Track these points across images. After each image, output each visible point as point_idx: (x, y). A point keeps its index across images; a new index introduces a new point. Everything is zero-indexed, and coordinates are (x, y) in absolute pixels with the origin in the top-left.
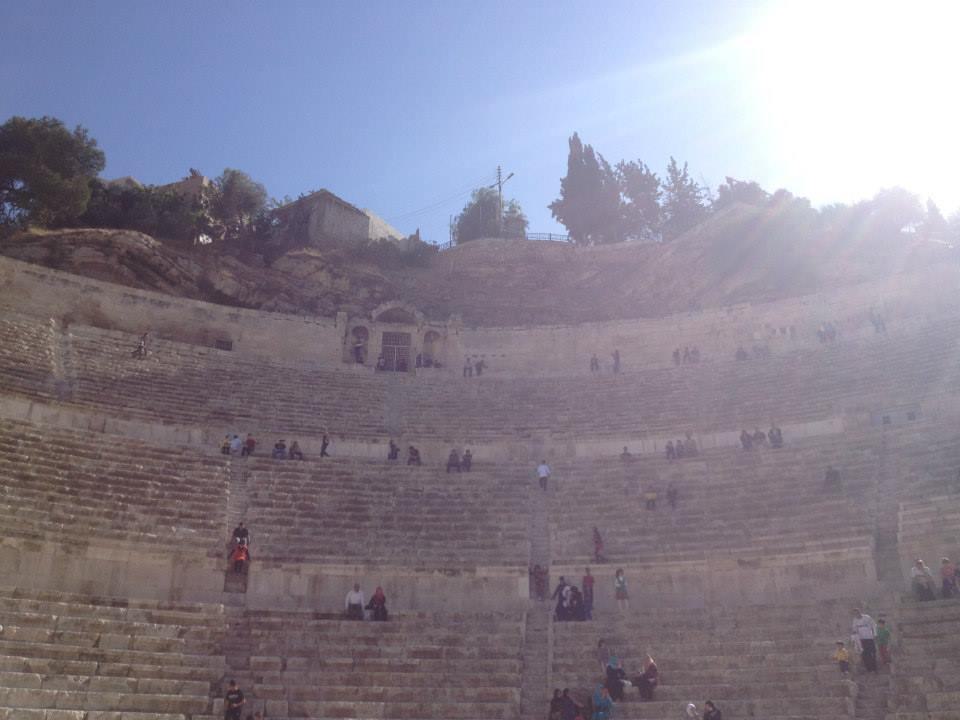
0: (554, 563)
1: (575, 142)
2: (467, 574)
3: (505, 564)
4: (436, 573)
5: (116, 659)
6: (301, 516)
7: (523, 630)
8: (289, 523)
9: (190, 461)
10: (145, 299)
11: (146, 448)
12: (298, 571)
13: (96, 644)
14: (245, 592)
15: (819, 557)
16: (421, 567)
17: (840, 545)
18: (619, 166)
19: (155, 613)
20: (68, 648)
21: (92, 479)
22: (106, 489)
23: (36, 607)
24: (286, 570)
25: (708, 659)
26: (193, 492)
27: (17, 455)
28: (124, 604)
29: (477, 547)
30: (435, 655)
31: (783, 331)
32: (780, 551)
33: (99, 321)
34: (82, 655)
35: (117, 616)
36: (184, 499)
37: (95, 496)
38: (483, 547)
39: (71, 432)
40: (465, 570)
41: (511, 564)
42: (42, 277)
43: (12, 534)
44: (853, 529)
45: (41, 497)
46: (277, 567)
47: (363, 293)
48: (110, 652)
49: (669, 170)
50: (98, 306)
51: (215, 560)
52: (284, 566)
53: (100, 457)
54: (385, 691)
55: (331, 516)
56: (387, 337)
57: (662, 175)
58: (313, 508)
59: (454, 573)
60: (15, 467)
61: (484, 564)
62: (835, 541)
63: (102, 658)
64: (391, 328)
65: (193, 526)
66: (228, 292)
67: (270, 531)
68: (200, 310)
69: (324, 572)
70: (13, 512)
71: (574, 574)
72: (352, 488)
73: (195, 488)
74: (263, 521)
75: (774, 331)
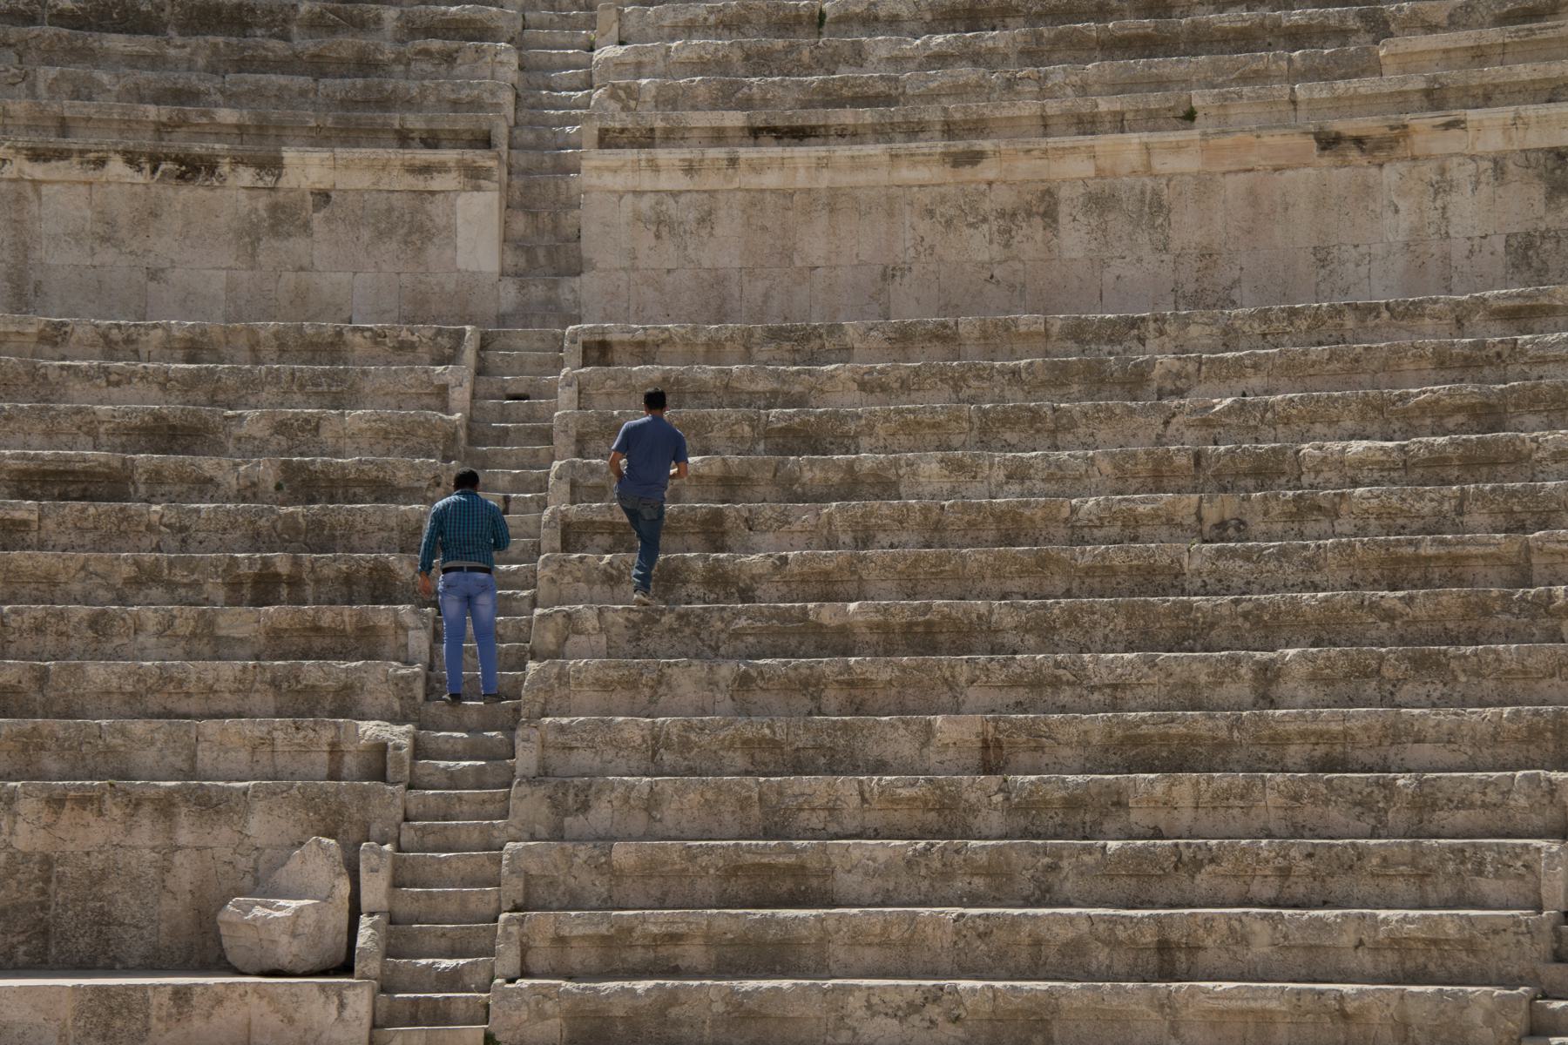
0: (606, 140)
2: (247, 176)
3: (404, 139)
4: (117, 167)
7: (460, 395)
16: (54, 141)
25: (1143, 504)
29: (284, 66)
30: (113, 486)
32: (1487, 98)
38: (318, 67)
41: (431, 141)
59: (193, 169)
61: (320, 138)
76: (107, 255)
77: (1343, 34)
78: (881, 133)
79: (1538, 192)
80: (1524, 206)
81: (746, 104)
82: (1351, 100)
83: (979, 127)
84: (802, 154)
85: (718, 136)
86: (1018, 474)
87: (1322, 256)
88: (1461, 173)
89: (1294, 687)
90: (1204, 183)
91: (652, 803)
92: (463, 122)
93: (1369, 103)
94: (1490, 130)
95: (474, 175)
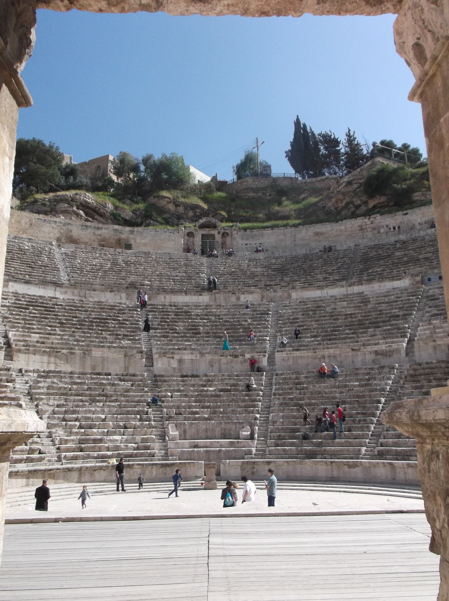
0: (278, 351)
1: (297, 123)
2: (241, 357)
3: (257, 352)
4: (229, 357)
5: (111, 396)
6: (172, 333)
8: (167, 337)
9: (123, 310)
10: (91, 227)
11: (105, 305)
12: (173, 358)
13: (103, 391)
14: (153, 366)
15: (383, 347)
17: (393, 342)
18: (319, 135)
19: (122, 377)
20: (94, 393)
21: (86, 321)
22: (93, 326)
23: (79, 378)
24: (168, 357)
25: (333, 390)
26: (127, 324)
27: (56, 313)
28: (109, 374)
29: (245, 345)
30: (229, 391)
31: (394, 228)
32: (369, 345)
33: (72, 240)
34: (99, 395)
35: (108, 379)
36: (123, 328)
37: (90, 329)
39: (74, 300)
40: (241, 355)
42: (45, 220)
43: (63, 349)
44: (399, 335)
45: (69, 331)
46: (165, 356)
47: (191, 214)
48: (109, 393)
49: (347, 135)
50: (71, 232)
51: (140, 354)
52: (167, 356)
53: (87, 311)
54: (210, 405)
55: (184, 333)
56: (203, 236)
57: (342, 138)
58: (176, 329)
59: (236, 356)
60: (57, 319)
62: (391, 340)
63: (106, 396)
64: (206, 231)
65: (129, 340)
66: (127, 218)
67: (160, 341)
68: (116, 230)
69: (183, 358)
70: (61, 339)
71: (285, 356)
72: (192, 319)
73: (127, 323)
74: (156, 336)
75: (390, 229)
76: (228, 366)
77: (355, 338)
78: (306, 350)
79: (374, 355)
80: (373, 356)
81: (292, 347)
82: (356, 346)
83: (317, 349)
84: (298, 352)
85: (289, 351)
86: (320, 387)
87: (353, 362)
88: (367, 353)
89: (347, 409)
90: (340, 354)
91: (283, 422)
92: (263, 350)
93: (357, 346)
94: (369, 348)
95: (264, 356)
